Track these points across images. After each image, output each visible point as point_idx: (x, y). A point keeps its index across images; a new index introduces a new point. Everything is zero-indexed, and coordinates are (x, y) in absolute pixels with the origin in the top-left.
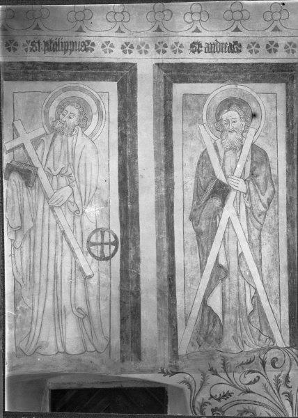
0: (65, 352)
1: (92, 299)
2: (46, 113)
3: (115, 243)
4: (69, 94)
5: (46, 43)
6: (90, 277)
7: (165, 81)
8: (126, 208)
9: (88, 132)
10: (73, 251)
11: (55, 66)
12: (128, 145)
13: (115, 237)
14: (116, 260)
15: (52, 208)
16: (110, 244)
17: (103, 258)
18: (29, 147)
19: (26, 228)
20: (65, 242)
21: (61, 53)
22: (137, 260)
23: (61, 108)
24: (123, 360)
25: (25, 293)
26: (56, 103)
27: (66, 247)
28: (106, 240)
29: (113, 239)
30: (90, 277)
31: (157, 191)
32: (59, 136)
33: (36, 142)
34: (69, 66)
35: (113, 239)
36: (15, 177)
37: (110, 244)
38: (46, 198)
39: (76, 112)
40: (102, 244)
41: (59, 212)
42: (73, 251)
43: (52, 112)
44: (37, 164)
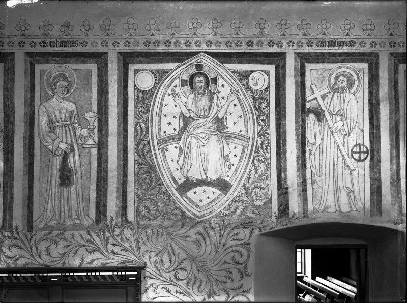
0: (340, 211)
1: (355, 183)
2: (329, 81)
3: (367, 152)
4: (343, 70)
5: (329, 42)
6: (353, 170)
7: (395, 63)
8: (373, 133)
9: (352, 91)
10: (343, 156)
11: (334, 55)
12: (374, 98)
13: (367, 148)
14: (368, 161)
15: (332, 133)
16: (364, 152)
17: (360, 160)
18: (320, 100)
19: (318, 144)
20: (339, 151)
21: (337, 48)
22: (379, 161)
23: (337, 78)
24: (372, 216)
25: (318, 179)
26: (334, 75)
27: (340, 154)
28: (362, 150)
29: (365, 150)
30: (353, 170)
31: (390, 123)
32: (336, 93)
33: (324, 97)
34: (341, 54)
35: (365, 150)
36: (312, 116)
37: (364, 152)
38: (329, 127)
39: (345, 80)
40: (360, 152)
41: (335, 134)
42: (343, 156)
43: (332, 81)
44: (324, 108)
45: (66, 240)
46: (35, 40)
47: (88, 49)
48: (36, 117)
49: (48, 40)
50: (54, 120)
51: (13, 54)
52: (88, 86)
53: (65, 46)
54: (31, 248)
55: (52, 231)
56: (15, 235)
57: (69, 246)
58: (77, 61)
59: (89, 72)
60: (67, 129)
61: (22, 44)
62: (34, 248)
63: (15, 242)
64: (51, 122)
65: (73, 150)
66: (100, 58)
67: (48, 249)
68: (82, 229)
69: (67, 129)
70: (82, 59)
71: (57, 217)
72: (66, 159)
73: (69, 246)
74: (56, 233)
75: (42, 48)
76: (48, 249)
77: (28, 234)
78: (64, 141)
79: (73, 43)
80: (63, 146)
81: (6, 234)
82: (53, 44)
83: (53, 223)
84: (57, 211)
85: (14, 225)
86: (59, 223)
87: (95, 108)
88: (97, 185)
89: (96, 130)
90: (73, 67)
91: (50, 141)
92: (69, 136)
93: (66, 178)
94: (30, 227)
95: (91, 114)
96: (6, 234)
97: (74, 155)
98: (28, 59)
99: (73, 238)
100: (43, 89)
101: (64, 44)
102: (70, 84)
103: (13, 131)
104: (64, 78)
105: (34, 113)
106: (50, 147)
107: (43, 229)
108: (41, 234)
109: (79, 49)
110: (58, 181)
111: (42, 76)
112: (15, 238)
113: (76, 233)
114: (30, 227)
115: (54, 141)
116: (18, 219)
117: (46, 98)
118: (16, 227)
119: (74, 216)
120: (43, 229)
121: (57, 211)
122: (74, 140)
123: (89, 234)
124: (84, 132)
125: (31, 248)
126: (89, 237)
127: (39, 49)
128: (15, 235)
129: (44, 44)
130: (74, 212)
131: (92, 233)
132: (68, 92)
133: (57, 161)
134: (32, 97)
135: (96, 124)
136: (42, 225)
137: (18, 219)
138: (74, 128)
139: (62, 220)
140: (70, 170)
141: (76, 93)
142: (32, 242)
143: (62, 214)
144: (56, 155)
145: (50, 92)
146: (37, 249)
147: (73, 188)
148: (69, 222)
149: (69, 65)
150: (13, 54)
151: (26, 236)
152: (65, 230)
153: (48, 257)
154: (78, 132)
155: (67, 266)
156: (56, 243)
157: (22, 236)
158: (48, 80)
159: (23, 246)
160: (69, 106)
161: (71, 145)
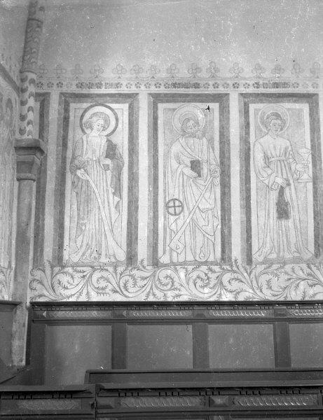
45: (286, 273)
46: (248, 82)
47: (300, 90)
48: (251, 153)
49: (261, 82)
50: (270, 155)
51: (227, 95)
52: (300, 124)
53: (277, 87)
54: (251, 282)
55: (272, 264)
56: (235, 268)
57: (290, 279)
58: (289, 101)
59: (301, 110)
60: (283, 165)
61: (236, 86)
62: (254, 282)
63: (236, 275)
64: (266, 158)
65: (289, 185)
66: (130, 98)
67: (268, 282)
68: (302, 263)
69: (283, 165)
70: (294, 98)
71: (276, 250)
72: (283, 194)
73: (290, 279)
74: (275, 266)
75: (256, 89)
76: (268, 282)
77: (248, 267)
78: (280, 175)
79: (285, 85)
80: (280, 181)
81: (225, 267)
82: (265, 86)
83: (274, 256)
84: (276, 244)
85: (233, 258)
86: (278, 256)
87: (309, 145)
88: (314, 218)
89: (310, 165)
90: (286, 107)
91: (265, 175)
92: (284, 171)
93: (283, 211)
94: (249, 260)
95: (304, 150)
96: (225, 267)
97: (290, 189)
98: (242, 98)
99: (293, 272)
100: (257, 128)
101: (276, 85)
102: (284, 122)
103: (229, 166)
104: (277, 116)
105: (249, 149)
106: (266, 182)
107: (263, 263)
108: (260, 268)
109: (290, 90)
110: (276, 215)
111: (256, 115)
112: (235, 272)
113: (297, 267)
114: (249, 260)
115: (269, 176)
116: (237, 252)
117: (260, 134)
118: (236, 260)
119: (293, 249)
120: (263, 263)
121: (276, 244)
122: (289, 173)
123: (309, 267)
124: (299, 167)
125: (251, 282)
126: (309, 271)
127: (251, 90)
128: (235, 268)
129: (257, 85)
130: (292, 245)
131: (312, 266)
132: (281, 129)
133: (274, 196)
134: (248, 133)
135: (310, 160)
136: (261, 259)
137: (237, 252)
138: (289, 164)
139: (281, 254)
140: (287, 204)
141: (290, 130)
142: (252, 275)
143: (281, 246)
144: (272, 189)
145: (264, 130)
146: (257, 282)
147: (291, 220)
148: (288, 256)
149: (281, 104)
150: (227, 95)
151: (246, 270)
152: (285, 263)
153: (270, 291)
154: (293, 167)
155: (289, 299)
156: (277, 275)
157: (242, 270)
158: (262, 118)
159: (243, 280)
160: (282, 143)
161: (287, 180)
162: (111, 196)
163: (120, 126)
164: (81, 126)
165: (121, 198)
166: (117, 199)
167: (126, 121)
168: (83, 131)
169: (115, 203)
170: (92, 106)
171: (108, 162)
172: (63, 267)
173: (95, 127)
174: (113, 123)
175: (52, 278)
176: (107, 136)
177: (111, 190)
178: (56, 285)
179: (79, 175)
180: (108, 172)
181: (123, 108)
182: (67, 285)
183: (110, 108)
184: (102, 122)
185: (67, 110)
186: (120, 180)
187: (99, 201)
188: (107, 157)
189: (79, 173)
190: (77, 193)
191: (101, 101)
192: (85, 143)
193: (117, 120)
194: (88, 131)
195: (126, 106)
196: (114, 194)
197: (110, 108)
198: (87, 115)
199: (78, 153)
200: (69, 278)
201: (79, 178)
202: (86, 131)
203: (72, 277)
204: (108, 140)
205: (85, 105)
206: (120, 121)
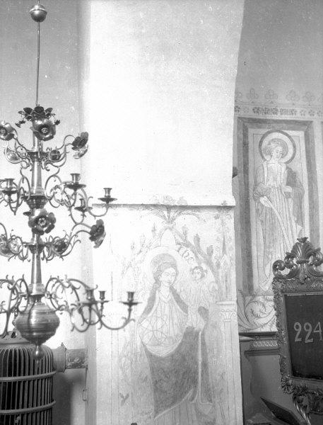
162: (294, 224)
163: (298, 152)
164: (261, 152)
165: (303, 225)
166: (299, 227)
167: (303, 148)
168: (263, 157)
169: (298, 231)
170: (269, 133)
171: (289, 189)
172: (254, 296)
173: (274, 154)
174: (291, 151)
175: (245, 309)
176: (287, 163)
177: (294, 219)
178: (249, 315)
179: (263, 203)
180: (290, 200)
181: (299, 134)
182: (259, 313)
183: (287, 135)
184: (280, 149)
185: (245, 136)
186: (301, 208)
187: (283, 228)
188: (287, 184)
189: (263, 200)
190: (262, 222)
191: (277, 127)
192: (266, 169)
193: (294, 147)
194: (267, 158)
195: (301, 134)
196: (297, 222)
197: (287, 135)
198: (265, 143)
199: (260, 179)
200: (261, 307)
201: (262, 206)
202: (265, 157)
203: (264, 305)
204: (287, 168)
205: (263, 131)
206: (298, 148)
